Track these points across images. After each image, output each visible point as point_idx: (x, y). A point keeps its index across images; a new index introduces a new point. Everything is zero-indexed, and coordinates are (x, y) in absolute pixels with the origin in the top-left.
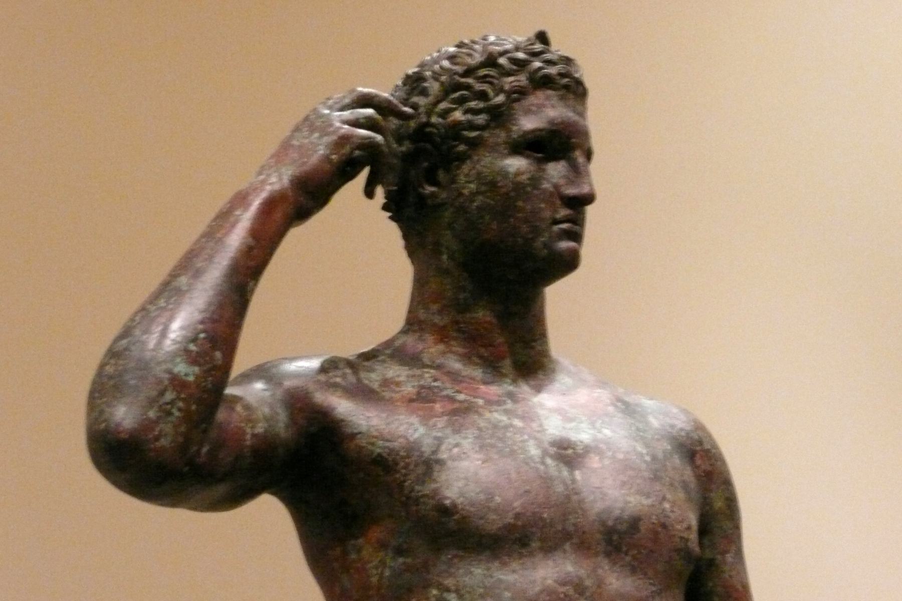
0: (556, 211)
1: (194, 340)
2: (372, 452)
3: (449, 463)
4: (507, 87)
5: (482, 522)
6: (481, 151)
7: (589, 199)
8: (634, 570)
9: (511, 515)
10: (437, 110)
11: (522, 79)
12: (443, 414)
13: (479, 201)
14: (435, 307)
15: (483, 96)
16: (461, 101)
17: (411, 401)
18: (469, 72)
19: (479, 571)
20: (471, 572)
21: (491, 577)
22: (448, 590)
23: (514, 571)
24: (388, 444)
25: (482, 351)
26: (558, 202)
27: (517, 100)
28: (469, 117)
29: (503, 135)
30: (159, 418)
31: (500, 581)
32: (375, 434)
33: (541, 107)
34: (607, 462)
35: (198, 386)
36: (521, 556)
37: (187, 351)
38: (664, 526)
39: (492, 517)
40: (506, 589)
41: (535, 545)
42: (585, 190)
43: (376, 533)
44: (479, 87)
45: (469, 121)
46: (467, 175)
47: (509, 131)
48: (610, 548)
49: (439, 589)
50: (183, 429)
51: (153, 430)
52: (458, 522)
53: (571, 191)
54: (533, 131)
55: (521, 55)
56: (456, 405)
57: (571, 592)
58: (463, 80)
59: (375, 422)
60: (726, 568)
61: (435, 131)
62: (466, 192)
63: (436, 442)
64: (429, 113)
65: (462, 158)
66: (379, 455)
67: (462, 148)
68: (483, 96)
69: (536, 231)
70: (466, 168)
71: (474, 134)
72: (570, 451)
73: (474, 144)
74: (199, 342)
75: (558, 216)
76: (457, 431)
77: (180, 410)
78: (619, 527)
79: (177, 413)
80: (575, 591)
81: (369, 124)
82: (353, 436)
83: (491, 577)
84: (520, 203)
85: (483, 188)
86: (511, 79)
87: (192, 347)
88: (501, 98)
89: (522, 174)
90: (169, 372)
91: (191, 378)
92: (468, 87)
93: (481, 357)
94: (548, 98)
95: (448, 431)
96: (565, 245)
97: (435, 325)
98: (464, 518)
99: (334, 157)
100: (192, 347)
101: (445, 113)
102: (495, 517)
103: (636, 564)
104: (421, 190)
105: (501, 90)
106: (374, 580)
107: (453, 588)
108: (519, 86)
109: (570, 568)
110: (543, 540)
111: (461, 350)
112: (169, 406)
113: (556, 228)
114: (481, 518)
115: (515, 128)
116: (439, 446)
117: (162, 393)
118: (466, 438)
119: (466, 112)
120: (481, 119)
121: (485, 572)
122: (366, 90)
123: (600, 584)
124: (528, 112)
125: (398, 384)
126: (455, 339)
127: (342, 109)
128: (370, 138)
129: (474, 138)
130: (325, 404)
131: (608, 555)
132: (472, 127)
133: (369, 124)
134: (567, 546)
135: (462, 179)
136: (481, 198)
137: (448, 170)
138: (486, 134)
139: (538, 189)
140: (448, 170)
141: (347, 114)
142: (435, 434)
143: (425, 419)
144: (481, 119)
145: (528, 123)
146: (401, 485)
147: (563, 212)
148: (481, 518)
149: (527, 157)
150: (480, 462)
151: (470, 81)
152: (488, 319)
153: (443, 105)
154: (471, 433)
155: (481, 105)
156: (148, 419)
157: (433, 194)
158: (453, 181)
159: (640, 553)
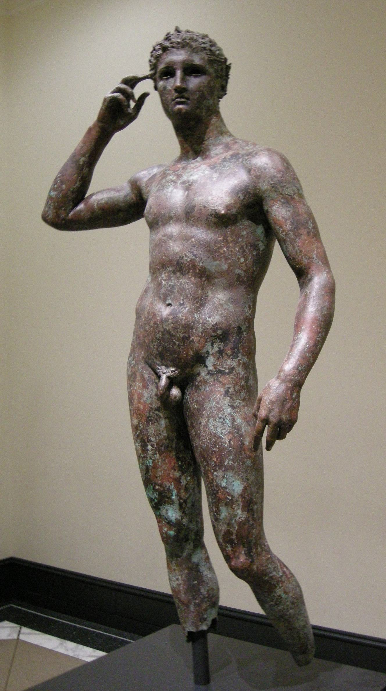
9: (153, 214)
38: (205, 207)
41: (160, 224)
60: (273, 213)
75: (174, 98)
77: (52, 206)
91: (54, 196)
103: (193, 223)
110: (162, 221)
134: (171, 222)
159: (195, 219)
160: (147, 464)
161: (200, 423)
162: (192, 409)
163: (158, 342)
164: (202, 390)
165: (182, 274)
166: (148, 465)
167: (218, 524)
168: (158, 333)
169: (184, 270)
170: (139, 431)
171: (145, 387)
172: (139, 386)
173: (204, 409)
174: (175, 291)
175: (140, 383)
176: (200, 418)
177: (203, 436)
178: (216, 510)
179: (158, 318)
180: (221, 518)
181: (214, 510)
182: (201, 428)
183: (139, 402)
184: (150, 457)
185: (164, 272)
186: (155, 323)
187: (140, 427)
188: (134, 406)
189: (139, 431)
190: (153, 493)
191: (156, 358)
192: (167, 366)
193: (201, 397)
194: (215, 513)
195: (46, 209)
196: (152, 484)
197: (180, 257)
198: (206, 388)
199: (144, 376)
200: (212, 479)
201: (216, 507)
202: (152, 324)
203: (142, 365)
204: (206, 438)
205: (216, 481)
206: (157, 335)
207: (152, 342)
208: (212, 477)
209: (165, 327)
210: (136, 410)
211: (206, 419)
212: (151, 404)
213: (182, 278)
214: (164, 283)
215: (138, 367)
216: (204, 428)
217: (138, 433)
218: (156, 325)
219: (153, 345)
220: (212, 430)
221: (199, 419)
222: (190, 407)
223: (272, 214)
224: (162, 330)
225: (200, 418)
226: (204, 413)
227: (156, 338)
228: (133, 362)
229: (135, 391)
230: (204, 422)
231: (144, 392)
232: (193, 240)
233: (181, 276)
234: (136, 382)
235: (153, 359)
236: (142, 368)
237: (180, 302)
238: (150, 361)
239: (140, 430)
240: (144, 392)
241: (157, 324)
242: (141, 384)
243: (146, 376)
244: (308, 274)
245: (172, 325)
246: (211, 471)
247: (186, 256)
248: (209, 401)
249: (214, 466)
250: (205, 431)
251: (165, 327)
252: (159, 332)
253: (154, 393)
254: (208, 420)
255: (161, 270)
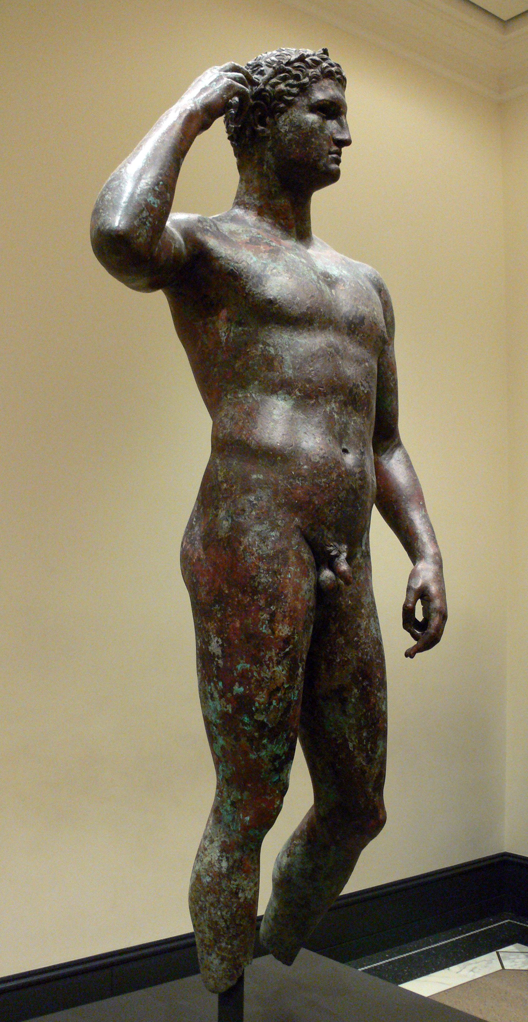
0: (331, 147)
1: (158, 184)
2: (228, 268)
3: (272, 278)
4: (310, 74)
5: (290, 310)
6: (294, 108)
7: (347, 143)
8: (360, 344)
10: (270, 82)
11: (317, 71)
12: (265, 252)
13: (290, 136)
14: (255, 196)
15: (297, 77)
16: (284, 79)
17: (247, 243)
18: (289, 63)
19: (286, 336)
20: (282, 337)
21: (293, 340)
22: (269, 345)
23: (305, 338)
24: (236, 265)
25: (282, 221)
26: (332, 142)
27: (315, 82)
28: (288, 88)
29: (306, 101)
30: (139, 226)
31: (297, 341)
32: (231, 258)
33: (326, 88)
34: (347, 287)
35: (159, 211)
36: (309, 330)
37: (154, 189)
39: (296, 307)
40: (301, 347)
41: (316, 325)
42: (346, 137)
43: (224, 314)
44: (294, 72)
45: (288, 91)
46: (284, 121)
47: (309, 99)
48: (350, 332)
49: (263, 344)
50: (150, 234)
51: (136, 233)
52: (276, 309)
53: (339, 137)
54: (323, 100)
55: (317, 59)
56: (272, 248)
57: (333, 351)
58: (287, 67)
59: (229, 252)
61: (268, 94)
62: (282, 130)
63: (263, 265)
64: (265, 84)
65: (282, 112)
66: (232, 270)
67: (282, 105)
68: (297, 77)
69: (320, 156)
70: (283, 117)
71: (290, 98)
72: (329, 279)
73: (290, 104)
74: (160, 186)
76: (274, 261)
77: (150, 222)
78: (354, 321)
79: (149, 225)
80: (335, 351)
81: (240, 81)
82: (218, 259)
83: (293, 340)
84: (313, 140)
85: (293, 129)
86: (312, 70)
87: (156, 188)
88: (306, 80)
89: (315, 123)
90: (146, 200)
91: (156, 206)
92: (289, 72)
93: (281, 225)
94: (329, 84)
95: (270, 261)
96: (334, 166)
97: (255, 205)
98: (280, 307)
99: (224, 96)
100: (156, 188)
101: (277, 84)
102: (296, 308)
103: (362, 341)
104: (255, 128)
105: (307, 75)
106: (224, 339)
107: (272, 344)
108: (316, 74)
109: (332, 339)
110: (320, 323)
111: (270, 221)
112: (145, 220)
113: (330, 156)
114: (290, 308)
115: (313, 97)
116: (265, 268)
117: (141, 212)
118: (279, 265)
119: (286, 86)
120: (295, 90)
121: (289, 337)
122: (237, 64)
123: (345, 348)
124: (320, 89)
125: (239, 234)
126: (267, 213)
127: (226, 71)
128: (242, 88)
129: (291, 100)
130: (203, 239)
131: (348, 335)
132: (289, 94)
133: (240, 81)
135: (281, 123)
136: (291, 134)
137: (272, 116)
138: (297, 99)
139: (323, 133)
140: (272, 116)
141: (230, 74)
142: (262, 261)
143: (256, 254)
144: (295, 90)
145: (319, 96)
146: (244, 288)
147: (334, 148)
148: (290, 308)
149: (318, 115)
150: (288, 278)
151: (290, 68)
152: (286, 204)
153: (274, 80)
154: (282, 263)
155: (295, 83)
156: (134, 226)
157: (263, 131)
158: (275, 123)
160: (290, 698)
161: (359, 626)
162: (344, 607)
163: (339, 504)
164: (357, 579)
165: (355, 409)
166: (291, 701)
167: (370, 768)
168: (342, 491)
169: (359, 404)
170: (291, 646)
171: (305, 574)
172: (295, 573)
173: (362, 606)
174: (349, 432)
175: (296, 568)
176: (358, 619)
177: (365, 643)
178: (371, 747)
179: (343, 469)
180: (377, 757)
181: (369, 747)
182: (361, 633)
183: (297, 599)
184: (297, 686)
185: (333, 400)
186: (339, 475)
187: (294, 638)
188: (287, 604)
189: (291, 646)
190: (283, 745)
191: (329, 529)
192: (340, 543)
193: (357, 589)
194: (370, 752)
195: (136, 223)
196: (286, 731)
197: (354, 385)
198: (360, 576)
199: (303, 557)
200: (374, 705)
201: (372, 743)
202: (334, 476)
203: (296, 539)
204: (369, 647)
205: (378, 705)
206: (339, 494)
207: (330, 503)
208: (374, 701)
209: (351, 483)
210: (291, 611)
211: (366, 620)
212: (308, 601)
213: (356, 415)
214: (336, 416)
215: (290, 543)
216: (365, 632)
217: (287, 650)
218: (341, 479)
219: (330, 508)
220: (374, 634)
221: (356, 621)
222: (342, 605)
223: (388, 354)
224: (348, 487)
225: (358, 619)
226: (363, 611)
227: (338, 498)
228: (273, 534)
229: (288, 581)
230: (364, 624)
231: (303, 581)
232: (367, 364)
233: (354, 412)
234: (289, 566)
235: (323, 531)
236: (298, 544)
237: (361, 450)
238: (314, 534)
239: (293, 644)
240: (303, 581)
241: (342, 477)
242: (299, 570)
243: (306, 556)
244: (396, 438)
245: (360, 482)
246: (374, 693)
247: (362, 385)
248: (366, 594)
249: (378, 684)
250: (367, 637)
251: (351, 483)
252: (343, 489)
253: (312, 583)
254: (369, 621)
255: (329, 397)
